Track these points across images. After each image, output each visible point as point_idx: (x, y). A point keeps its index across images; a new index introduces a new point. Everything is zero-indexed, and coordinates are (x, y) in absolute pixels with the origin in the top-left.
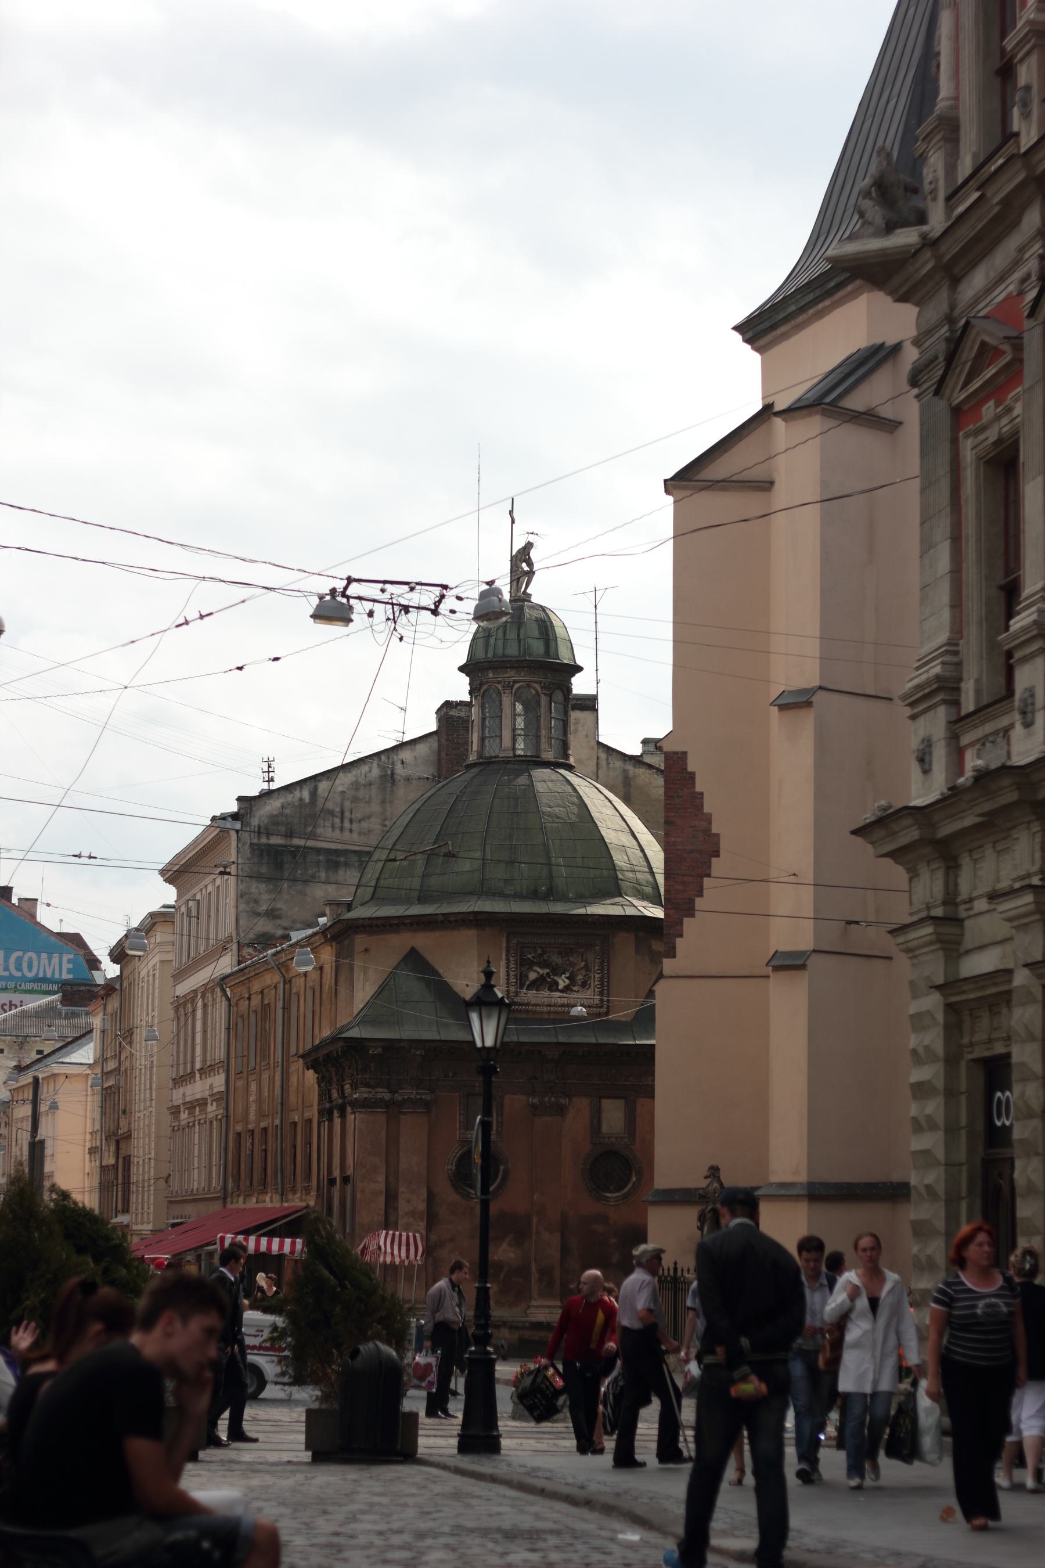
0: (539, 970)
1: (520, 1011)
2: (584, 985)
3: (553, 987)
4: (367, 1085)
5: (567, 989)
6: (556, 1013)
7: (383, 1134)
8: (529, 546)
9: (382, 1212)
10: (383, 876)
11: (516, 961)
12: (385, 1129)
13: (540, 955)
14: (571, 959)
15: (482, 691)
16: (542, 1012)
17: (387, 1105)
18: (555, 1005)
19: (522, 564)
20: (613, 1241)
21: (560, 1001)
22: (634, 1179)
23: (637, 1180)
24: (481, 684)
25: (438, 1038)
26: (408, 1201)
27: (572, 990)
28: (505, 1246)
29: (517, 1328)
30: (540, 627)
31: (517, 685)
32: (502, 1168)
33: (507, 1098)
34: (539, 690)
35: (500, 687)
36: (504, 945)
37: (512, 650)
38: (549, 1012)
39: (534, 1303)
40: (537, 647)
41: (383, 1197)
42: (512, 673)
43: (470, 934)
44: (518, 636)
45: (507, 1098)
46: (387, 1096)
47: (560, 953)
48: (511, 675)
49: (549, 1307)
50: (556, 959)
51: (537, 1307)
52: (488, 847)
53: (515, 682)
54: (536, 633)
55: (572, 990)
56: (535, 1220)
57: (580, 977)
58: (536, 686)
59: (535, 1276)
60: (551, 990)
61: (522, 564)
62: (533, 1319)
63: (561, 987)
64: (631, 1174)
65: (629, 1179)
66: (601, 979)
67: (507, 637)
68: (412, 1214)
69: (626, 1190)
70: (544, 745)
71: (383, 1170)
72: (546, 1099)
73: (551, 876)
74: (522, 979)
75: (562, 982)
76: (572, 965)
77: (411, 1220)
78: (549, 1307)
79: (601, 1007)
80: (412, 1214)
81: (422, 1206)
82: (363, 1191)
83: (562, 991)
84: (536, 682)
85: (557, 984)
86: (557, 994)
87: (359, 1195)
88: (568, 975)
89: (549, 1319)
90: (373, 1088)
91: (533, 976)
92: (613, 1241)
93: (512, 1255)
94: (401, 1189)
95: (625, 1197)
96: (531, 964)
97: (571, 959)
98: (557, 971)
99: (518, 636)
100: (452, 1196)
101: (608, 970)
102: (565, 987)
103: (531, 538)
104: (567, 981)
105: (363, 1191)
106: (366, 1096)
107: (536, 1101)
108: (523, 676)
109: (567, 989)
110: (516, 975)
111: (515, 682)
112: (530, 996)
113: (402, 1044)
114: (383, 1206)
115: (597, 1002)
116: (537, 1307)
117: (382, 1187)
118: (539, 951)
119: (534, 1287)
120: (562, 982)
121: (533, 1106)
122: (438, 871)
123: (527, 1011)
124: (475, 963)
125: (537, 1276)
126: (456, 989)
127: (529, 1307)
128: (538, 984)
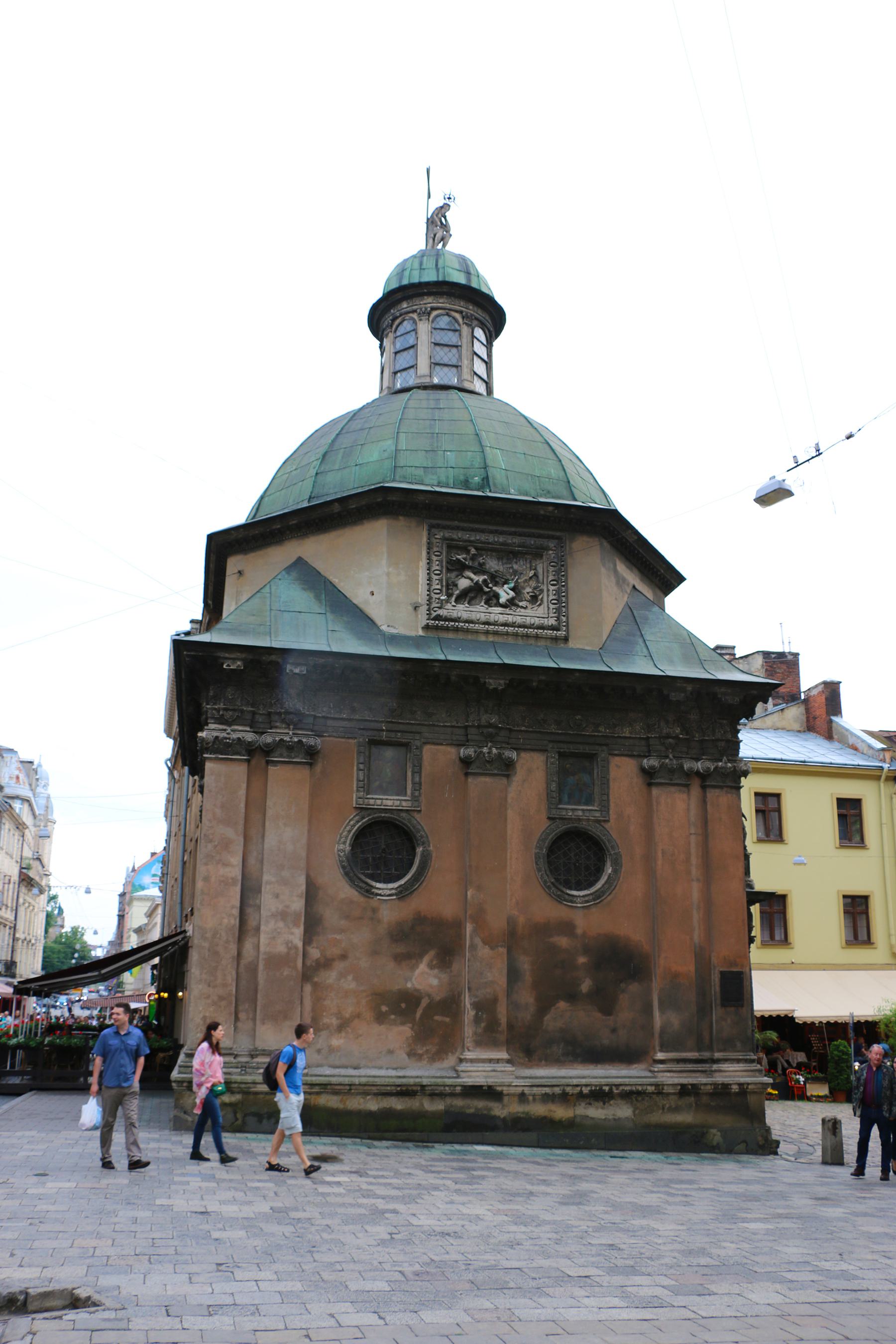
0: (472, 576)
1: (447, 629)
2: (534, 599)
3: (492, 599)
4: (221, 720)
5: (511, 603)
6: (496, 633)
7: (242, 792)
8: (444, 208)
9: (236, 912)
10: (268, 493)
11: (441, 561)
12: (244, 786)
13: (473, 558)
14: (515, 567)
15: (394, 326)
16: (477, 632)
17: (251, 751)
18: (495, 624)
19: (438, 225)
20: (582, 960)
21: (502, 619)
22: (610, 871)
23: (615, 871)
24: (393, 320)
25: (328, 649)
26: (277, 896)
27: (518, 606)
28: (423, 967)
29: (442, 1095)
30: (459, 262)
31: (435, 313)
32: (419, 850)
33: (427, 748)
34: (460, 320)
35: (415, 316)
36: (425, 540)
37: (430, 276)
38: (487, 633)
39: (469, 1055)
40: (460, 279)
41: (238, 889)
42: (430, 299)
43: (377, 531)
44: (437, 265)
45: (428, 751)
46: (250, 737)
47: (499, 559)
48: (429, 302)
49: (490, 1061)
50: (493, 565)
51: (472, 1061)
52: (402, 436)
53: (433, 309)
54: (457, 266)
55: (518, 606)
56: (469, 928)
57: (528, 590)
58: (457, 316)
59: (469, 1014)
60: (487, 602)
61: (438, 225)
62: (468, 1080)
63: (502, 600)
64: (603, 862)
65: (599, 871)
66: (558, 592)
67: (424, 266)
68: (283, 915)
69: (598, 885)
70: (466, 374)
71: (239, 849)
72: (485, 750)
73: (485, 467)
74: (450, 586)
75: (505, 594)
76: (515, 572)
77: (281, 924)
78: (490, 1061)
79: (558, 629)
80: (283, 915)
81: (298, 905)
82: (206, 879)
83: (502, 606)
84: (456, 311)
85: (497, 596)
86: (500, 610)
87: (200, 884)
88: (512, 585)
89: (490, 1081)
90: (230, 725)
91: (464, 583)
92: (582, 960)
93: (435, 982)
94: (266, 877)
95: (598, 895)
96: (460, 568)
97: (515, 567)
98: (495, 579)
99: (437, 265)
100: (345, 891)
101: (566, 581)
102: (508, 600)
103: (447, 201)
104: (512, 594)
105: (206, 879)
106: (215, 734)
107: (471, 751)
108: (442, 302)
109: (511, 603)
110: (441, 580)
111: (433, 309)
112: (462, 611)
113: (273, 658)
114: (238, 905)
115: (552, 622)
116: (472, 1061)
117: (237, 872)
118: (473, 551)
119: (469, 1031)
120: (505, 594)
121: (466, 762)
122: (337, 467)
123: (457, 630)
124: (384, 562)
125: (473, 1013)
126: (355, 602)
127: (461, 1061)
128: (469, 595)
